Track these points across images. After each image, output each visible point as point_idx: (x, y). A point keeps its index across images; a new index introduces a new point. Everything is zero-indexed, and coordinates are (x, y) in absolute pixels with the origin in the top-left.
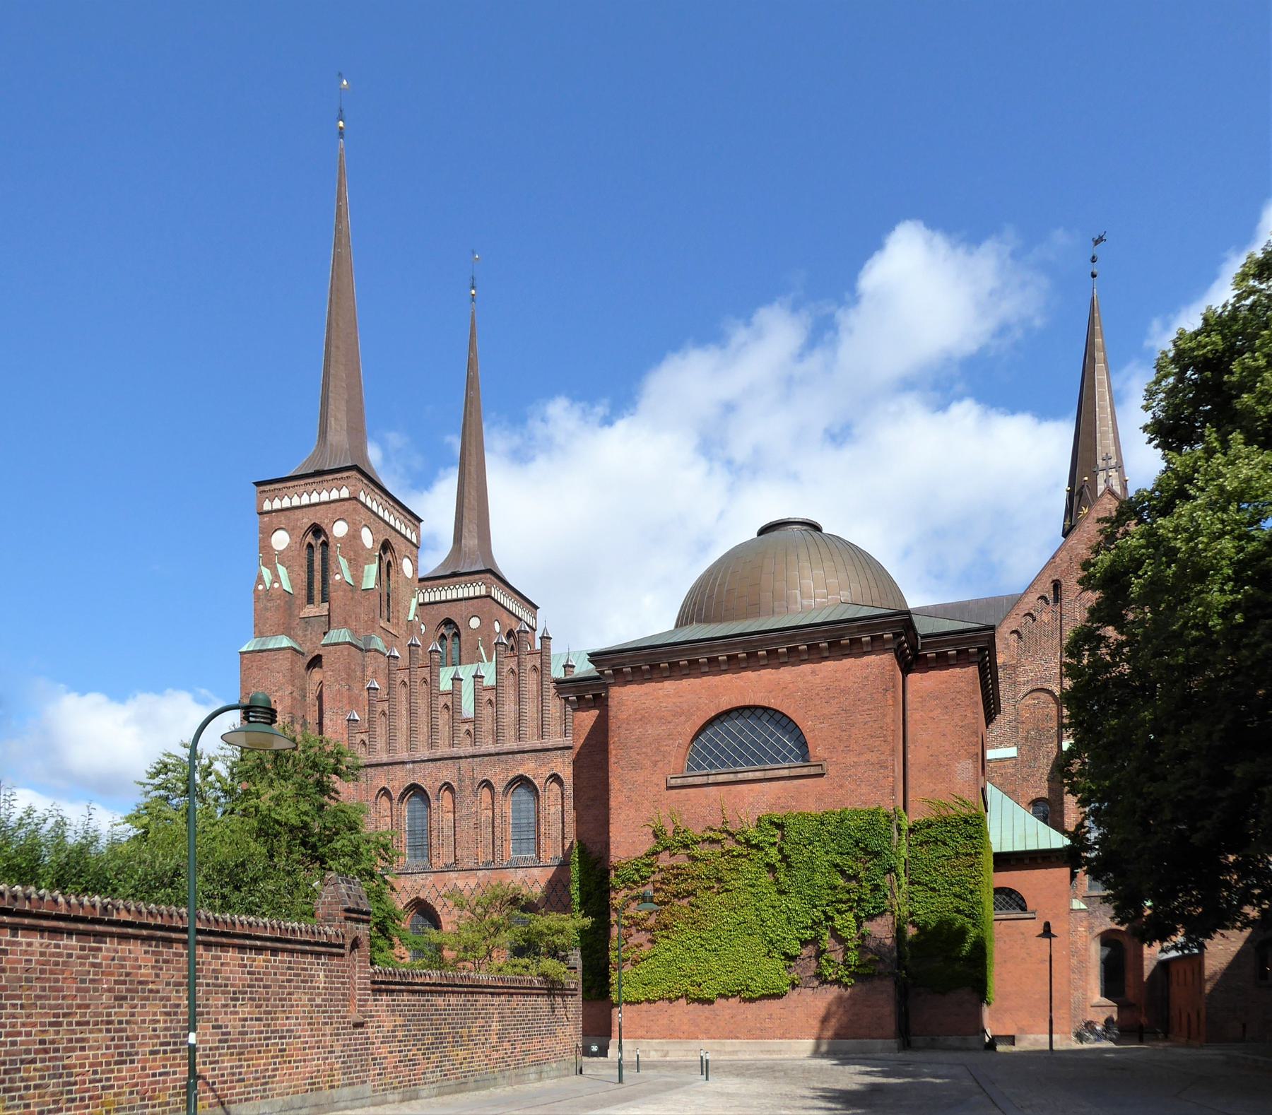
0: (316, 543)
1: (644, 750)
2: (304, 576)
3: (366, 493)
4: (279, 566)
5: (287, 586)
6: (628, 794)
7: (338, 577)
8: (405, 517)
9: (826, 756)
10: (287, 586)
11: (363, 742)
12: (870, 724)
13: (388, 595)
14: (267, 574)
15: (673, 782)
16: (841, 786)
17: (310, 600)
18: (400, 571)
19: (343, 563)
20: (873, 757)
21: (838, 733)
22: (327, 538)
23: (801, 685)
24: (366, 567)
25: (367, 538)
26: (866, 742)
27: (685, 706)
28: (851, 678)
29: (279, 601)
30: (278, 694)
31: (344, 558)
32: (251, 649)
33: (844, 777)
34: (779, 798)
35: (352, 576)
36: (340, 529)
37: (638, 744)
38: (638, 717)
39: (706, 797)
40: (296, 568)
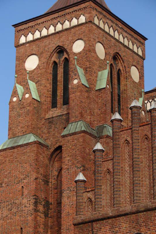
0: (59, 61)
2: (50, 87)
3: (100, 18)
4: (29, 81)
5: (35, 95)
7: (75, 82)
8: (132, 36)
10: (35, 95)
11: (90, 200)
13: (119, 96)
14: (20, 89)
17: (54, 105)
18: (129, 77)
19: (80, 71)
22: (69, 56)
24: (100, 73)
25: (100, 50)
29: (28, 108)
30: (25, 181)
31: (81, 67)
32: (5, 147)
35: (87, 80)
36: (78, 47)
40: (43, 82)
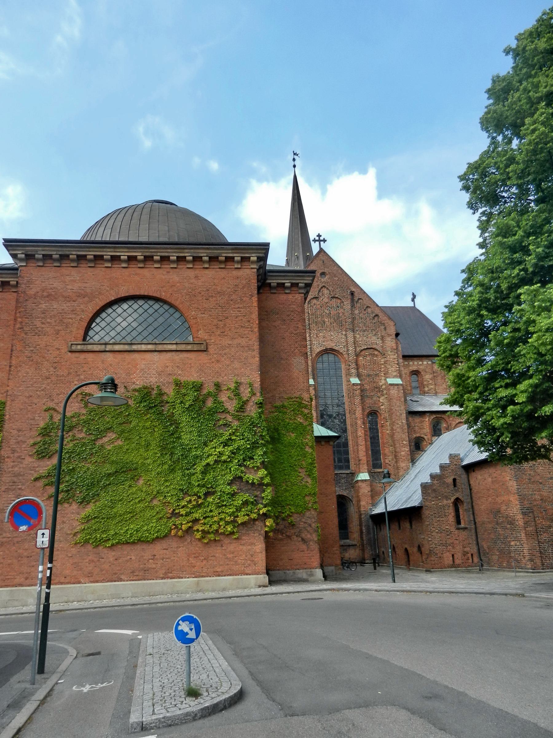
1: (49, 320)
6: (30, 355)
9: (206, 338)
12: (240, 318)
15: (74, 348)
16: (218, 361)
20: (243, 342)
21: (215, 321)
23: (187, 285)
26: (238, 331)
27: (88, 290)
28: (226, 284)
33: (220, 354)
34: (167, 367)
37: (43, 316)
38: (45, 294)
39: (103, 362)
